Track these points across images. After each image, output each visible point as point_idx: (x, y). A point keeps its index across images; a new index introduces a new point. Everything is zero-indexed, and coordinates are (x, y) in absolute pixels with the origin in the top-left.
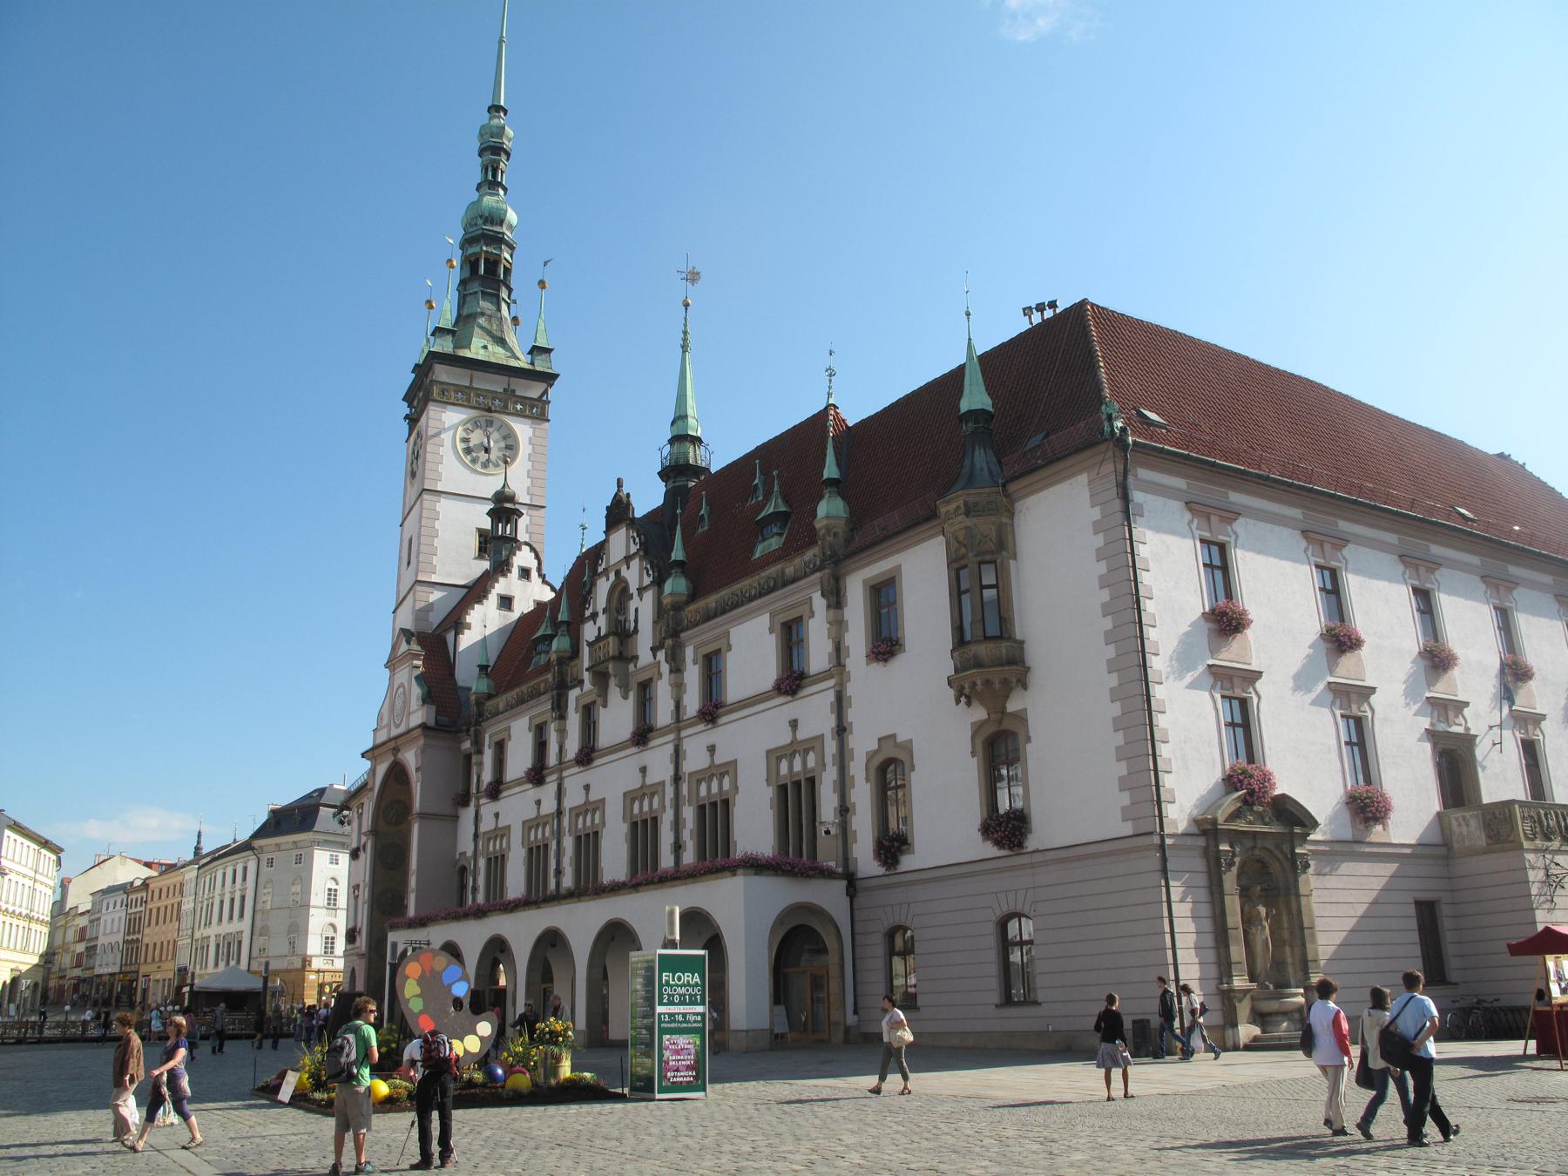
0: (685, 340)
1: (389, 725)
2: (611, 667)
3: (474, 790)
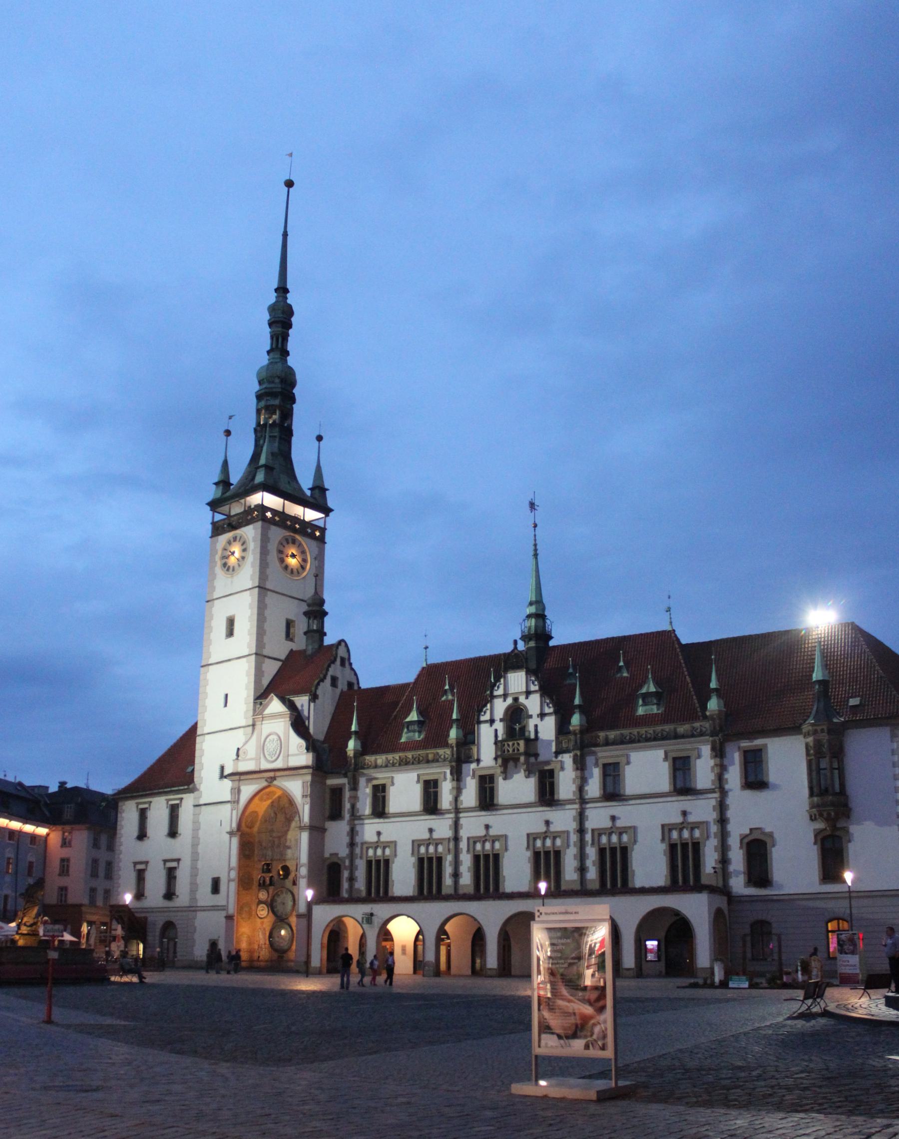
0: (536, 550)
1: (258, 760)
2: (522, 759)
3: (347, 816)
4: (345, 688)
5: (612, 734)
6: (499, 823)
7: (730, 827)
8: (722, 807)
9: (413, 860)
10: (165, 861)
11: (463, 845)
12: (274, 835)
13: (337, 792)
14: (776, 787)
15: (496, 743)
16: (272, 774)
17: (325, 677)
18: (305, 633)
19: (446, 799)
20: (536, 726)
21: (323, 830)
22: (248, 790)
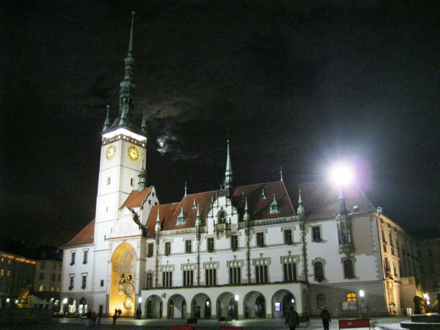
2: (225, 231)
4: (154, 205)
5: (260, 221)
6: (215, 256)
7: (308, 257)
8: (304, 249)
9: (182, 272)
10: (82, 274)
11: (201, 266)
12: (126, 262)
13: (151, 246)
14: (325, 241)
15: (214, 225)
16: (125, 238)
17: (146, 200)
18: (139, 183)
19: (194, 247)
20: (230, 219)
21: (145, 261)
22: (116, 245)
